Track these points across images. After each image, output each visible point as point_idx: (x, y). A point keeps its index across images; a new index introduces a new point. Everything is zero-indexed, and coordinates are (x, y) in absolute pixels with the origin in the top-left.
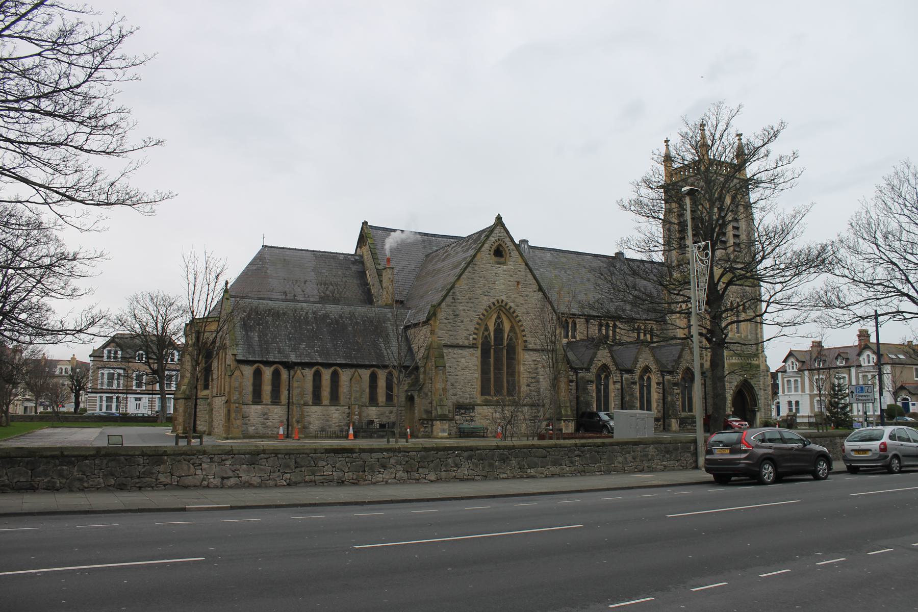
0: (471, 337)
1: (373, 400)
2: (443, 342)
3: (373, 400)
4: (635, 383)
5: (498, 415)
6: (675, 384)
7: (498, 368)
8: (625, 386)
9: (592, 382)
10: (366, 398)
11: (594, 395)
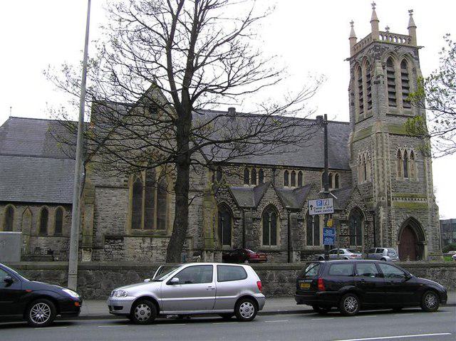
0: (122, 180)
1: (43, 230)
2: (95, 184)
3: (43, 230)
4: (302, 220)
5: (146, 245)
6: (343, 222)
7: (149, 204)
8: (291, 222)
9: (259, 219)
10: (36, 230)
11: (261, 230)
